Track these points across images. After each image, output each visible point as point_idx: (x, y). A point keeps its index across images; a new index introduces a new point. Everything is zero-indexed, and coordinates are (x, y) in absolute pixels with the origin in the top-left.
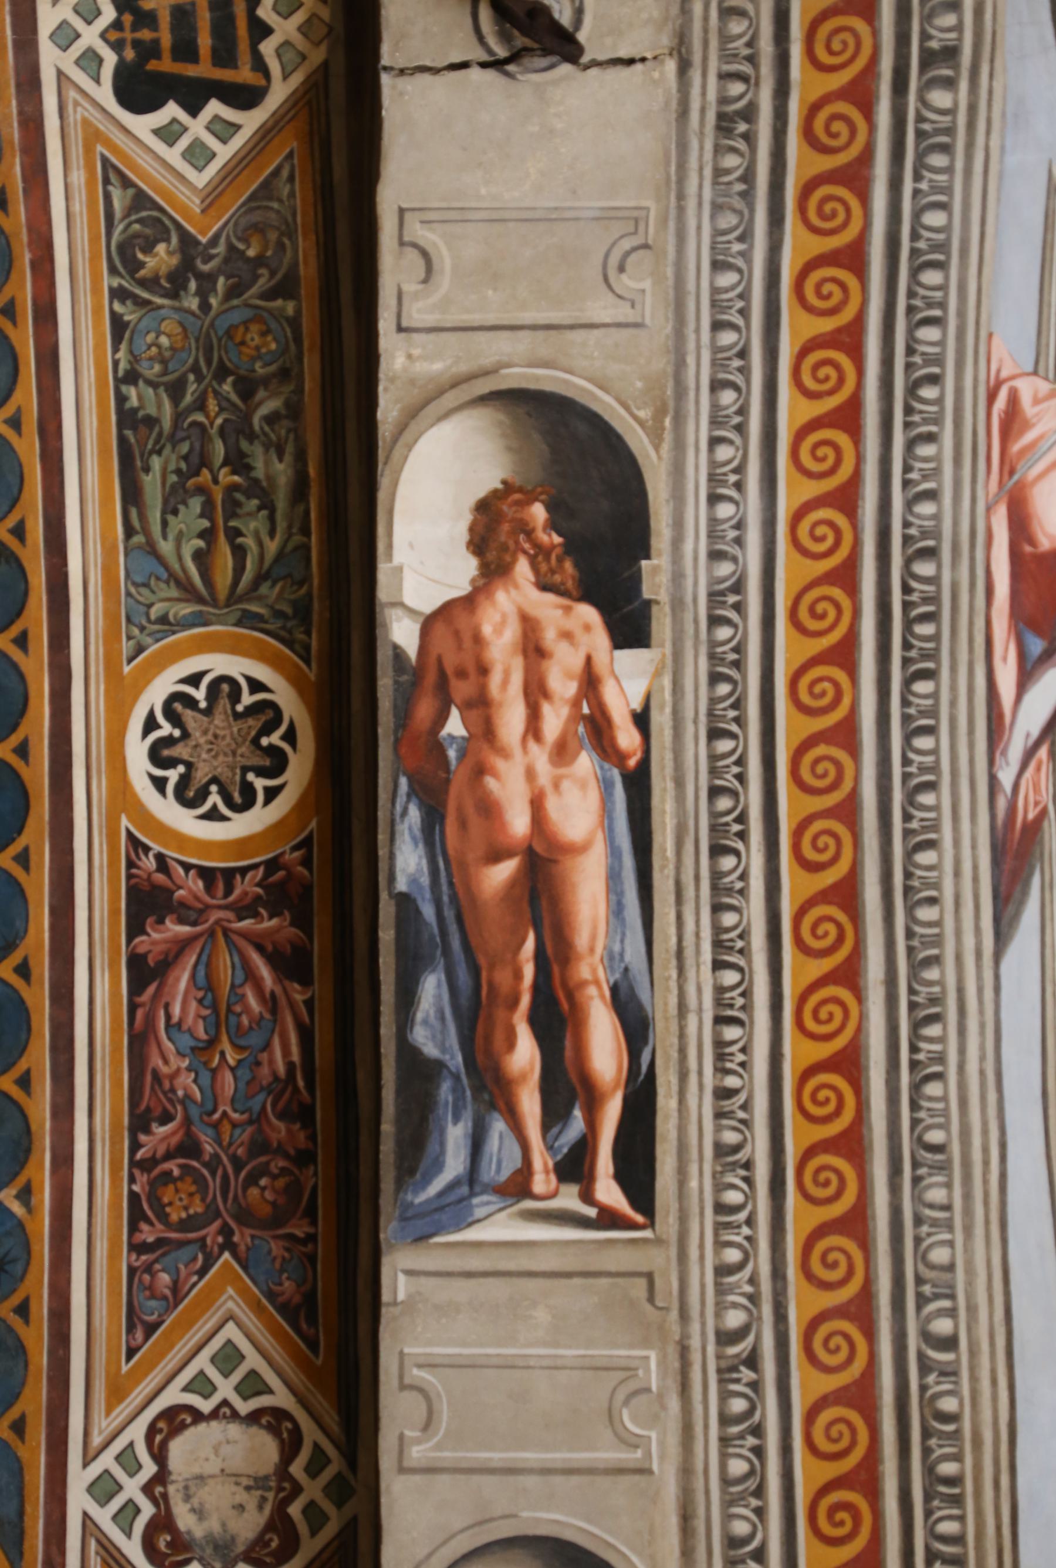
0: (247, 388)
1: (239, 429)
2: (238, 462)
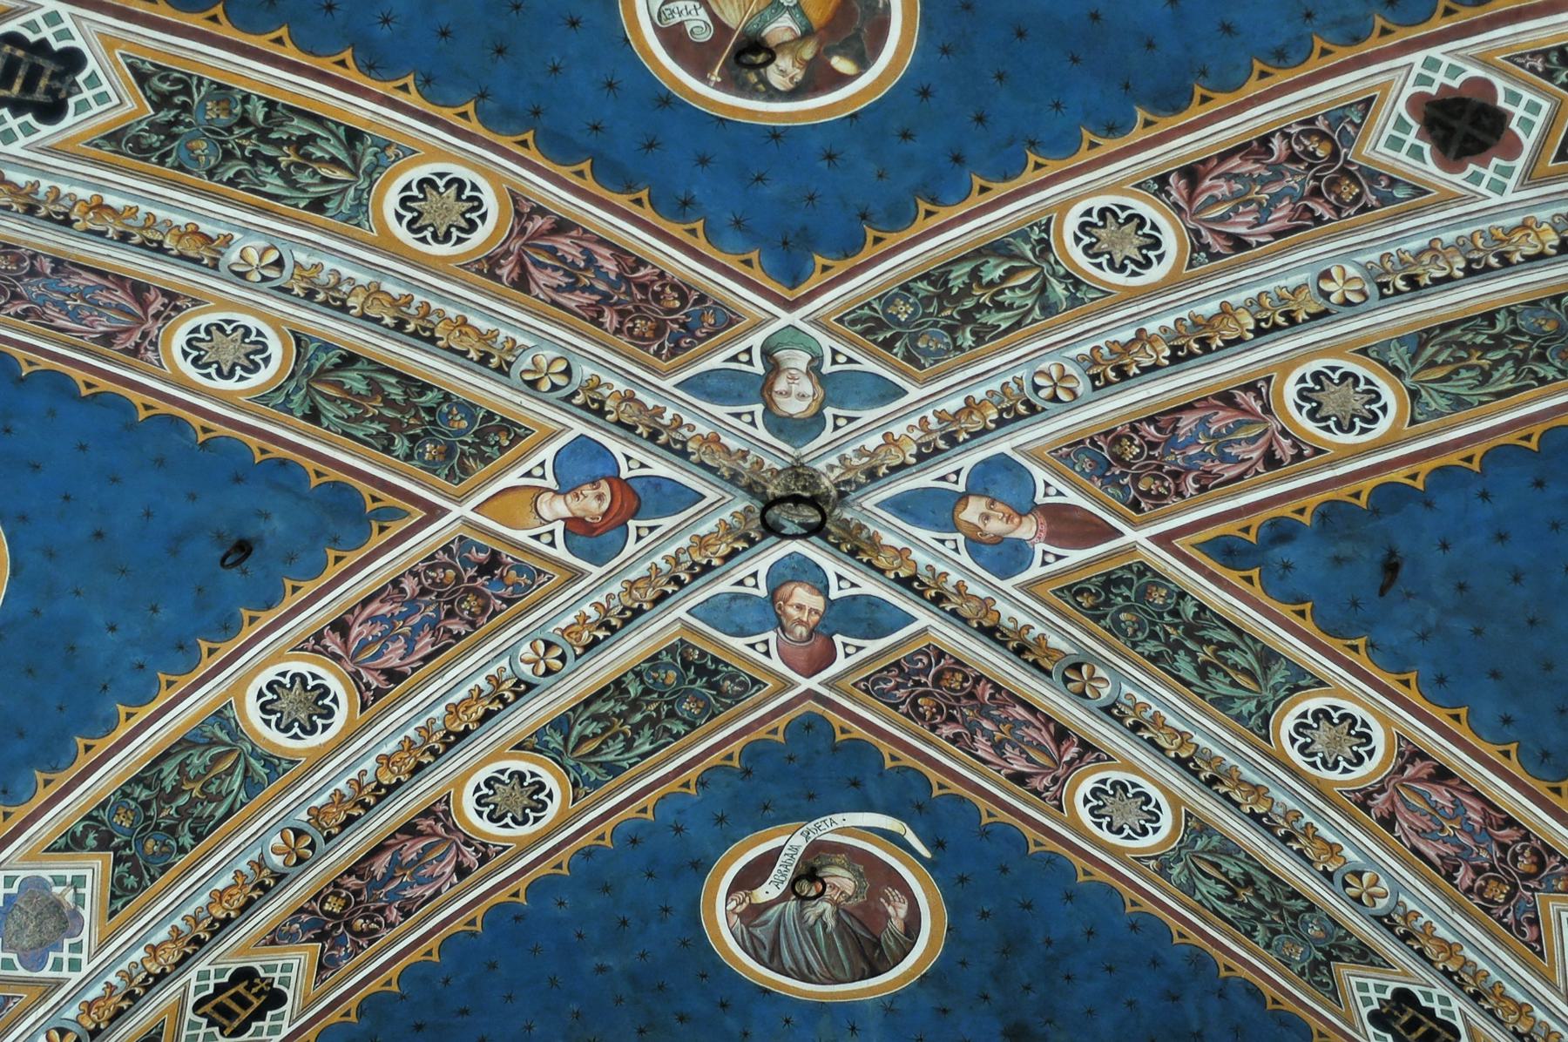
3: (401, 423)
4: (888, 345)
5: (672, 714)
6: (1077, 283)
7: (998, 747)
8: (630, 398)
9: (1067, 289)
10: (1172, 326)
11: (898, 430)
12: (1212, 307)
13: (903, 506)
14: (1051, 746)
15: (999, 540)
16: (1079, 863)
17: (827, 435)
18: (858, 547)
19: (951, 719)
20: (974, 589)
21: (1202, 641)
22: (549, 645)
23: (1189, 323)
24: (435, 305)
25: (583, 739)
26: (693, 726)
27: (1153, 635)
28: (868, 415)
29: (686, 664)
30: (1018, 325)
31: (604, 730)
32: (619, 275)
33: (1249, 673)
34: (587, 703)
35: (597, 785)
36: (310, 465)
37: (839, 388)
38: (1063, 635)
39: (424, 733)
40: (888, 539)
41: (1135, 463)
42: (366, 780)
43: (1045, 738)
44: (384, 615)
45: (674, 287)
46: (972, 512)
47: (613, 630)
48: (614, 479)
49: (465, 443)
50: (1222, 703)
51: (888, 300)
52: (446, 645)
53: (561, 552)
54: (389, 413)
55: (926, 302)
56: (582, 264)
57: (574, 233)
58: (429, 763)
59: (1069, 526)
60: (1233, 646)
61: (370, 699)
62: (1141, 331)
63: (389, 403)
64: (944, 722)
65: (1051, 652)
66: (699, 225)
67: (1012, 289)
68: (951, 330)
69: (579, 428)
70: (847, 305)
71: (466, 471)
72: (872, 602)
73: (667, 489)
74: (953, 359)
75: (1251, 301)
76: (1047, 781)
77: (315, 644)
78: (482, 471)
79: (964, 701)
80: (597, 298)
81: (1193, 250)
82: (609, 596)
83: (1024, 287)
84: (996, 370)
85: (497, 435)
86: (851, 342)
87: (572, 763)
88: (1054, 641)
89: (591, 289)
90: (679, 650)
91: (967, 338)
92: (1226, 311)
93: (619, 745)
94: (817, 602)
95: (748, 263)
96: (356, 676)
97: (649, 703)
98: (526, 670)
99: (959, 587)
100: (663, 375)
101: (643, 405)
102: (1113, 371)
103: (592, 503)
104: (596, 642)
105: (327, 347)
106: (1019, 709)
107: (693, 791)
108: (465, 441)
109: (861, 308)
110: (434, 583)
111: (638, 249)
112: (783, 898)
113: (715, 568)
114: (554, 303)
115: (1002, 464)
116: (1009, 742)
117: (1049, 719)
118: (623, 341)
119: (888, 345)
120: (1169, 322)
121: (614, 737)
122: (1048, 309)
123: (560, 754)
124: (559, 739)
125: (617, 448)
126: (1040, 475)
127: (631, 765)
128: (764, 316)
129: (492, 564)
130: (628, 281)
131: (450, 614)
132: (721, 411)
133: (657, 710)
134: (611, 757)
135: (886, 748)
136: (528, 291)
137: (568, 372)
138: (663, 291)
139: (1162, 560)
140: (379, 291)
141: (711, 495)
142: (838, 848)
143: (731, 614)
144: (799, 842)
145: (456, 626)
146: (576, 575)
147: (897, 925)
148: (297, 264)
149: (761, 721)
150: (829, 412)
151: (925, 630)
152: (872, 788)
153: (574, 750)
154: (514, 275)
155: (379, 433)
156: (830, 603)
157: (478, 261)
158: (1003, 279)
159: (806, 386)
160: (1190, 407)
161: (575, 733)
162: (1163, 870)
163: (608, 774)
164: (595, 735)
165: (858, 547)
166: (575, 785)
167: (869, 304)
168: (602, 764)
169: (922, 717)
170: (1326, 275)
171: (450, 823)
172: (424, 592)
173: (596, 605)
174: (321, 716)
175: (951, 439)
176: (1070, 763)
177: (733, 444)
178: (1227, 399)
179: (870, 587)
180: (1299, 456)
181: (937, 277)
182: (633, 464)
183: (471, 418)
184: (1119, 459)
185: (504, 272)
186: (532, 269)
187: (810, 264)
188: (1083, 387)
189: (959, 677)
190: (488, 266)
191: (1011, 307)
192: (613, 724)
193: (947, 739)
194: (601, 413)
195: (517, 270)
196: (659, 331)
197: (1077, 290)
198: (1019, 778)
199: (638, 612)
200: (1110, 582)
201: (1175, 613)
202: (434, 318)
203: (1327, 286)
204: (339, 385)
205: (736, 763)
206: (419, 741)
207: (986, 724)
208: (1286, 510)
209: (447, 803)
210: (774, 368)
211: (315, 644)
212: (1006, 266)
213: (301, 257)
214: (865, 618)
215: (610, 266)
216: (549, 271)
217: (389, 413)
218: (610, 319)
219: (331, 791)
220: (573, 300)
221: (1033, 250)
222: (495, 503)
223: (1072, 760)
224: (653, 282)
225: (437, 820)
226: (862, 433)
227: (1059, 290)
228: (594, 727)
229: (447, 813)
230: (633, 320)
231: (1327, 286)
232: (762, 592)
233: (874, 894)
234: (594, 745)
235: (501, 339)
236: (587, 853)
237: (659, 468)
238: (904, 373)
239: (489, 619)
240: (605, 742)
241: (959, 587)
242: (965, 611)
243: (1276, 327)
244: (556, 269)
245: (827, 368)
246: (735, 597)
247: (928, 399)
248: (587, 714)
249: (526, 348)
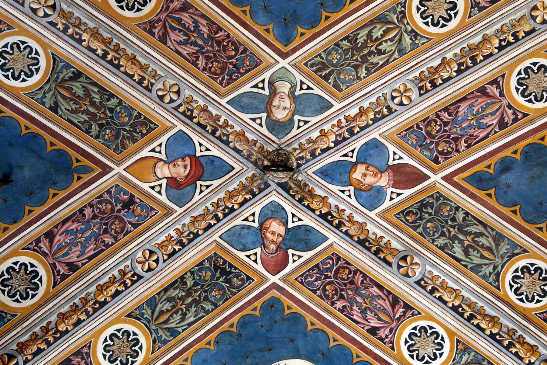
3: (96, 116)
4: (326, 78)
5: (206, 299)
6: (416, 35)
7: (363, 312)
8: (205, 110)
9: (411, 39)
10: (459, 53)
11: (327, 127)
12: (479, 38)
13: (324, 173)
14: (390, 309)
15: (371, 187)
17: (295, 132)
18: (303, 195)
19: (342, 297)
20: (358, 218)
21: (467, 233)
22: (152, 253)
23: (467, 49)
24: (122, 46)
25: (162, 313)
26: (216, 306)
27: (443, 234)
28: (314, 120)
29: (216, 268)
30: (387, 63)
31: (173, 307)
32: (209, 36)
33: (489, 249)
34: (166, 290)
35: (165, 342)
36: (49, 138)
37: (303, 104)
38: (397, 240)
39: (84, 301)
40: (318, 192)
41: (436, 136)
42: (50, 327)
43: (386, 305)
44: (73, 230)
45: (233, 43)
46: (357, 175)
47: (183, 245)
48: (193, 157)
49: (125, 130)
50: (476, 269)
51: (328, 52)
52: (102, 251)
53: (163, 198)
54: (92, 109)
55: (346, 52)
56: (192, 29)
57: (191, 11)
58: (84, 320)
59: (405, 177)
60: (482, 234)
61: (59, 280)
62: (444, 58)
63: (93, 104)
64: (338, 300)
65: (393, 252)
66: (247, 8)
67: (386, 41)
68: (356, 67)
69: (180, 126)
70: (310, 55)
71: (124, 147)
72: (308, 229)
73: (217, 164)
74: (357, 84)
75: (498, 31)
76: (387, 332)
77: (34, 247)
78: (132, 147)
79: (349, 286)
80: (197, 48)
81: (472, 7)
82: (184, 225)
83: (391, 40)
84: (376, 89)
85: (142, 127)
86: (310, 77)
87: (154, 328)
88: (395, 244)
89: (195, 44)
90: (214, 259)
91: (363, 73)
92: (486, 39)
93: (177, 317)
94: (281, 230)
95: (267, 30)
96: (54, 266)
97: (196, 291)
98: (139, 269)
99: (350, 217)
100: (222, 96)
101: (210, 113)
102: (429, 83)
103: (181, 171)
104: (174, 252)
105: (68, 66)
106: (375, 289)
107: (212, 347)
108: (125, 129)
109: (316, 57)
110: (100, 212)
111: (219, 21)
113: (235, 210)
114: (177, 52)
115: (375, 144)
116: (369, 309)
117: (389, 293)
118: (205, 76)
119: (326, 78)
120: (457, 51)
121: (176, 312)
122: (402, 52)
123: (149, 321)
124: (149, 312)
125: (196, 139)
126: (392, 148)
127: (183, 330)
128: (272, 61)
129: (129, 203)
130: (212, 38)
131: (106, 231)
132: (246, 117)
133: (199, 296)
134: (173, 325)
135: (309, 318)
136: (165, 44)
137: (178, 93)
138: (228, 45)
139: (448, 190)
140: (97, 33)
141: (237, 168)
143: (239, 238)
145: (108, 240)
146: (169, 212)
148: (62, 9)
149: (249, 303)
150: (296, 118)
151: (331, 245)
152: (300, 343)
153: (156, 319)
154: (161, 33)
155: (85, 121)
156: (288, 230)
157: (145, 23)
158: (382, 36)
159: (287, 103)
160: (465, 99)
161: (158, 309)
163: (171, 335)
164: (168, 311)
165: (303, 195)
166: (154, 342)
167: (320, 55)
168: (168, 329)
169: (327, 297)
170: (535, 8)
171: (89, 361)
172: (95, 217)
173: (177, 230)
174: (32, 289)
175: (352, 133)
176: (399, 319)
177: (251, 137)
178: (482, 91)
179: (308, 221)
180: (515, 120)
181: (351, 38)
182: (203, 149)
183: (130, 116)
184: (429, 134)
185: (156, 31)
186: (169, 30)
187: (295, 32)
188: (414, 95)
189: (347, 271)
190: (149, 27)
191: (384, 53)
192: (177, 304)
193: (339, 310)
194: (191, 118)
195: (162, 30)
196: (223, 69)
197: (416, 39)
198: (373, 331)
199: (197, 235)
200: (423, 205)
201: (454, 219)
202: (121, 53)
203: (534, 13)
204: (69, 90)
205: (234, 329)
206: (81, 305)
207: (359, 299)
208: (508, 153)
209: (89, 348)
210: (274, 92)
211: (34, 247)
212: (384, 28)
213: (64, 7)
214: (302, 238)
215: (205, 30)
216: (177, 32)
217: (92, 109)
218: (201, 62)
219: (31, 333)
220: (185, 50)
221: (397, 18)
222: (135, 166)
223: (400, 316)
224: (224, 40)
225: (83, 358)
226: (312, 128)
227: (407, 40)
228: (167, 306)
229: (88, 354)
230: (212, 63)
231: (534, 13)
232: (256, 225)
234: (166, 317)
235: (150, 69)
237: (215, 152)
238: (332, 95)
239: (124, 236)
240: (171, 316)
241: (350, 217)
242: (352, 232)
243: (509, 44)
244: (180, 31)
245: (298, 92)
246: (243, 227)
247: (343, 108)
248: (164, 298)
249: (161, 77)
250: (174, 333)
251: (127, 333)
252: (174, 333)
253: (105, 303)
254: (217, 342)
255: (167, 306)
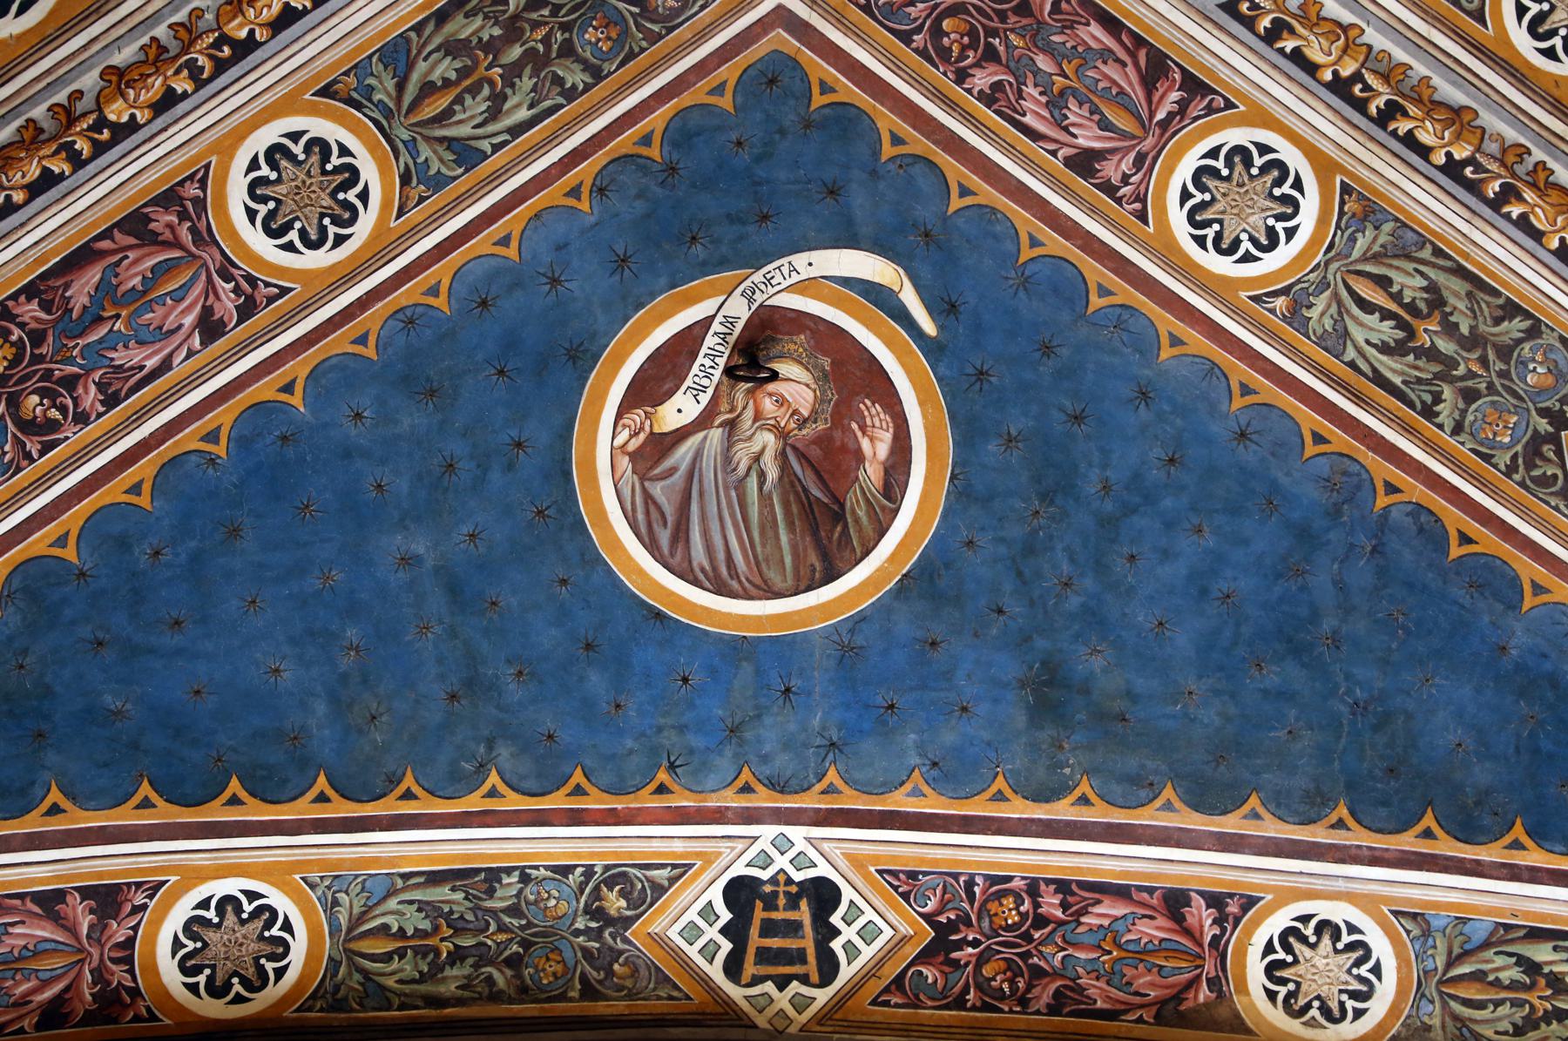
0: (514, 962)
1: (483, 956)
2: (457, 956)
5: (568, 50)
7: (1056, 103)
14: (1137, 93)
16: (1166, 322)
19: (991, 55)
26: (598, 75)
31: (463, 73)
35: (438, 183)
39: (183, 33)
42: (80, 107)
43: (1128, 80)
58: (185, 95)
64: (977, 65)
76: (1126, 166)
79: (1012, 19)
87: (405, 135)
93: (478, 106)
97: (536, 25)
106: (1095, 29)
107: (584, 206)
112: (703, 421)
116: (1074, 93)
117: (1139, 41)
121: (474, 90)
123: (389, 114)
124: (390, 84)
127: (496, 148)
133: (546, 41)
134: (465, 130)
135: (887, 120)
142: (800, 321)
144: (740, 309)
147: (872, 474)
149: (701, 69)
152: (858, 200)
153: (409, 111)
161: (415, 77)
162: (1296, 316)
163: (458, 163)
164: (447, 83)
166: (405, 179)
168: (449, 142)
169: (944, 54)
171: (202, 226)
176: (1164, 124)
192: (476, 63)
193: (981, 97)
198: (1084, 163)
205: (655, 152)
206: (174, 47)
207: (1043, 63)
209: (203, 184)
223: (1171, 116)
225: (183, 216)
228: (446, 68)
229: (200, 203)
233: (843, 413)
234: (443, 102)
236: (408, 319)
240: (459, 100)
248: (437, 41)
250: (466, 154)
251: (320, 146)
252: (466, 154)
253: (247, 46)
254: (600, 190)
255: (446, 68)
